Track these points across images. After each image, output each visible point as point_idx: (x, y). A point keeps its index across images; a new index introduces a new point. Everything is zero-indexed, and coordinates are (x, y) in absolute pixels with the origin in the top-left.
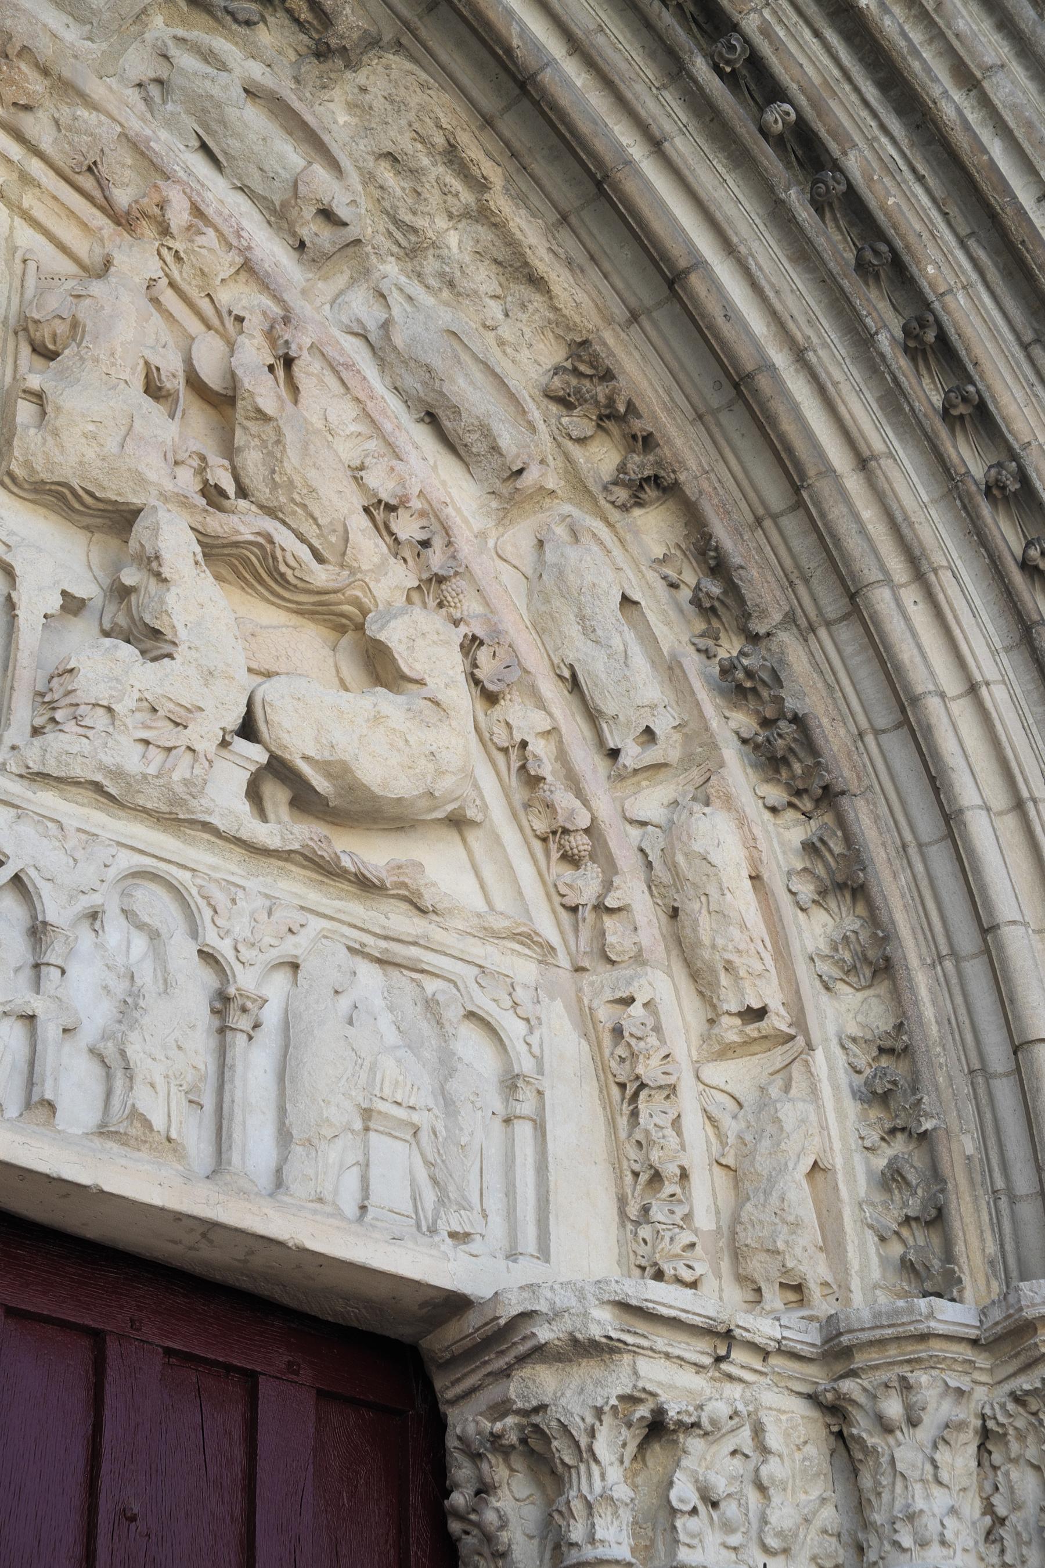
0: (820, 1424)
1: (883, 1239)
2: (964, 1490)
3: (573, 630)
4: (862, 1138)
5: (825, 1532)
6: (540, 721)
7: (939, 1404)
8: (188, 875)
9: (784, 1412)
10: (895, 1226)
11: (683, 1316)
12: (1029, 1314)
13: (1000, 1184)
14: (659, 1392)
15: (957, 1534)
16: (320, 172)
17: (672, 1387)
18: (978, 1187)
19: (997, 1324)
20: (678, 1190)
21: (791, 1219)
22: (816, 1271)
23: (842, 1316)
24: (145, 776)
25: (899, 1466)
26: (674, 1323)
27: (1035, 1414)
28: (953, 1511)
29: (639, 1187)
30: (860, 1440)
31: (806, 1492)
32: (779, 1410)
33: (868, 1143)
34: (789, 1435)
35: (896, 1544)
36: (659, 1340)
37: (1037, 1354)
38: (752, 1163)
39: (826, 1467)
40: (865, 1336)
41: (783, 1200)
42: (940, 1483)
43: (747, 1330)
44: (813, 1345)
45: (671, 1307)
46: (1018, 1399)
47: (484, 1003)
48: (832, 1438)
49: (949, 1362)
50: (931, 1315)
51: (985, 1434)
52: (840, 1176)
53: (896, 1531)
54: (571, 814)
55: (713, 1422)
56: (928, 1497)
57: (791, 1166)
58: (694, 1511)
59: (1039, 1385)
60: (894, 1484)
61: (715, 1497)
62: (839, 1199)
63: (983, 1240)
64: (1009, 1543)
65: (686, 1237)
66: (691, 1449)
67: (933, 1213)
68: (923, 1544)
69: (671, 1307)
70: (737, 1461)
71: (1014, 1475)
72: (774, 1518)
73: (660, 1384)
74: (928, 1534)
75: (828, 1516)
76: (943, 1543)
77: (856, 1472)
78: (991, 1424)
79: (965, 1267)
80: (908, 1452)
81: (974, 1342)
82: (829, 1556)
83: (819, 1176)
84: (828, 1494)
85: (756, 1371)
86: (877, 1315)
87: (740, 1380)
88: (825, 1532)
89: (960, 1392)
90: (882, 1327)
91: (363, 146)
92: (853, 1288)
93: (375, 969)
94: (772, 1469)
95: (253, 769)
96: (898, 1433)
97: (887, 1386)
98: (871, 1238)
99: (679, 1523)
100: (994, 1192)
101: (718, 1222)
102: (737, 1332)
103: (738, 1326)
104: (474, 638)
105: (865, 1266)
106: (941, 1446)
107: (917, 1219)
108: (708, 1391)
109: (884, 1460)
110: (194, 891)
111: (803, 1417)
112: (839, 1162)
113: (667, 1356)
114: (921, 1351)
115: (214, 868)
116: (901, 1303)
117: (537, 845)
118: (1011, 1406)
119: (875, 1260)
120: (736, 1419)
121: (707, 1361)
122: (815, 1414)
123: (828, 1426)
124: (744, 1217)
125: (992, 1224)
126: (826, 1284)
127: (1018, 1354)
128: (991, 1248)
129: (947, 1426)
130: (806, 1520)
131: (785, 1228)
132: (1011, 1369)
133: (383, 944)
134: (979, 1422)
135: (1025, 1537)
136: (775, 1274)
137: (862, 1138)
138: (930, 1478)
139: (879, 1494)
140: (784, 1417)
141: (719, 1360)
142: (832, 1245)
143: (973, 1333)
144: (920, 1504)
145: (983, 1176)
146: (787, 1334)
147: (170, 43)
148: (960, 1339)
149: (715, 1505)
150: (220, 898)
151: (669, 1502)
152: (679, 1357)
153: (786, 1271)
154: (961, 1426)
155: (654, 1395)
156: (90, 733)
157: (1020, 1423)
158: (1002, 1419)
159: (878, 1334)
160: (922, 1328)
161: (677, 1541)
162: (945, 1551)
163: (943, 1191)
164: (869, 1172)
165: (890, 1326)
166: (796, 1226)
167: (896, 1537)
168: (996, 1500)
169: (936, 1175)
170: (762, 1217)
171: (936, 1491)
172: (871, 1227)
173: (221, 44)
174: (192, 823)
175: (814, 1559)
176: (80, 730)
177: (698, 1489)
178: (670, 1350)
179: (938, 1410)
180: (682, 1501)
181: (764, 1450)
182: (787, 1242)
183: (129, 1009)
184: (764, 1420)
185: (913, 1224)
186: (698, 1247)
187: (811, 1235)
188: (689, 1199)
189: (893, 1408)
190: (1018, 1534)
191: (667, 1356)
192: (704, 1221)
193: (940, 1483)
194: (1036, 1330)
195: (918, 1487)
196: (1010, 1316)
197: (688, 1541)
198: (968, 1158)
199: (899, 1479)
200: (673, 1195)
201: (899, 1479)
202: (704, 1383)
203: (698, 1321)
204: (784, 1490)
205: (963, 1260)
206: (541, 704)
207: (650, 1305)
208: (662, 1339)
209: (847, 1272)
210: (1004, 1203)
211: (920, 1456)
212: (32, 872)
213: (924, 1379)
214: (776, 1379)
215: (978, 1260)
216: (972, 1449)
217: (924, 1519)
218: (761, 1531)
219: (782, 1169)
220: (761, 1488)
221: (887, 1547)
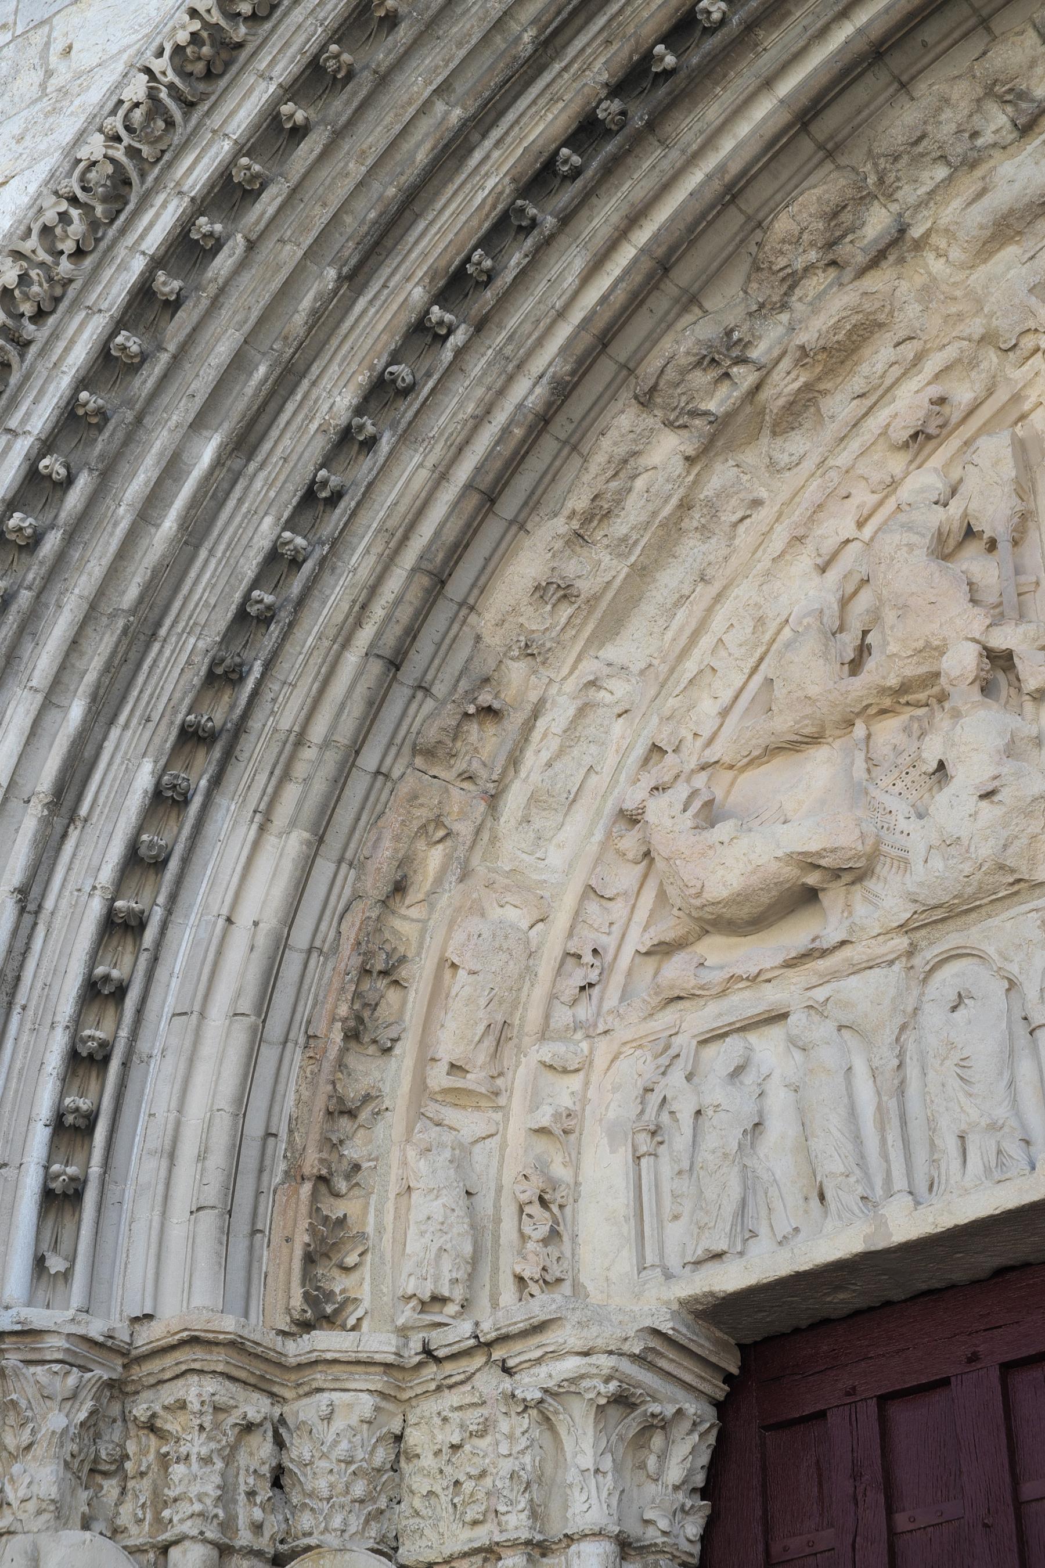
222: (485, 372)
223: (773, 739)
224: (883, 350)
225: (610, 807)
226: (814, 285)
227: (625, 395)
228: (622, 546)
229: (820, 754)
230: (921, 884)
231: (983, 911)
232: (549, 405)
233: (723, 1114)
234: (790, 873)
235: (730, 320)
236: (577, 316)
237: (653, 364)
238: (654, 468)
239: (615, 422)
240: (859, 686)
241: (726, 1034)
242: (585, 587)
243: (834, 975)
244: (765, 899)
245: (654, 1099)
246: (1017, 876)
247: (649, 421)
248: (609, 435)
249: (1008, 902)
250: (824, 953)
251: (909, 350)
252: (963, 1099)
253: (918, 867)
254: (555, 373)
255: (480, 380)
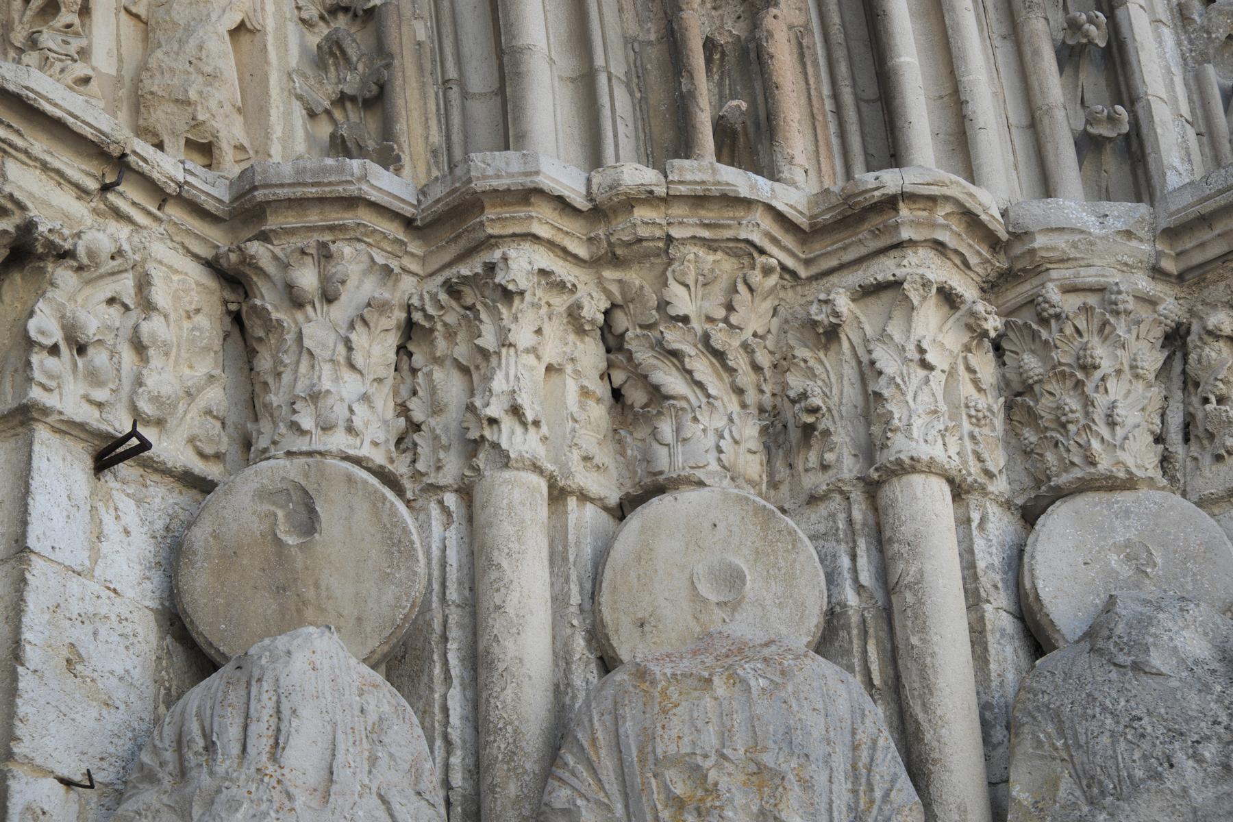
0: (216, 298)
1: (312, 115)
2: (379, 380)
4: (299, 8)
5: (209, 412)
7: (361, 281)
9: (176, 272)
10: (327, 104)
11: (70, 120)
12: (479, 185)
13: (452, 73)
14: (30, 205)
15: (367, 424)
17: (47, 204)
18: (427, 74)
19: (438, 201)
20: (75, 19)
21: (208, 69)
22: (230, 131)
23: (258, 169)
25: (307, 343)
26: (56, 127)
27: (471, 308)
28: (365, 398)
29: (29, 13)
30: (262, 313)
31: (191, 367)
32: (170, 267)
33: (305, 15)
34: (179, 298)
35: (295, 427)
36: (37, 145)
37: (482, 235)
38: (168, 12)
39: (217, 344)
40: (282, 193)
41: (201, 48)
42: (352, 366)
43: (145, 160)
44: (220, 201)
45: (56, 105)
46: (453, 290)
48: (228, 320)
49: (378, 237)
50: (364, 178)
51: (409, 329)
52: (270, 39)
53: (295, 412)
55: (91, 254)
56: (337, 379)
57: (214, 17)
58: (54, 350)
59: (479, 270)
60: (298, 362)
61: (83, 339)
62: (267, 62)
63: (427, 127)
64: (424, 449)
65: (80, 70)
66: (59, 282)
67: (374, 88)
68: (327, 428)
69: (56, 105)
70: (114, 311)
71: (438, 374)
72: (151, 381)
73: (31, 195)
74: (333, 416)
75: (215, 396)
76: (350, 429)
77: (250, 353)
78: (417, 317)
79: (405, 146)
80: (319, 329)
81: (408, 223)
82: (210, 440)
83: (245, 39)
84: (217, 372)
85: (149, 213)
86: (301, 171)
87: (129, 219)
88: (209, 412)
89: (387, 271)
90: (305, 184)
92: (273, 152)
94: (153, 327)
96: (309, 309)
97: (303, 253)
98: (298, 112)
99: (35, 359)
100: (445, 82)
101: (119, 70)
102: (132, 159)
103: (135, 152)
105: (288, 137)
106: (359, 327)
107: (353, 99)
108: (89, 222)
109: (290, 337)
111: (198, 284)
112: (270, 24)
113: (45, 167)
114: (348, 218)
116: (330, 162)
118: (443, 297)
119: (300, 134)
120: (119, 261)
121: (93, 185)
122: (211, 283)
123: (225, 303)
124: (153, 63)
125: (438, 115)
126: (240, 148)
127: (459, 236)
128: (436, 138)
129: (369, 305)
130: (189, 394)
131: (200, 79)
132: (447, 257)
134: (404, 315)
135: (444, 440)
136: (182, 126)
137: (299, 8)
138: (342, 359)
139: (279, 375)
140: (175, 278)
141: (106, 188)
142: (253, 108)
143: (409, 211)
144: (326, 384)
145: (434, 66)
146: (190, 179)
148: (394, 215)
149: (81, 349)
151: (26, 331)
152: (58, 172)
153: (196, 124)
154: (383, 307)
155: (22, 207)
157: (451, 319)
158: (431, 310)
159: (299, 192)
160: (352, 190)
161: (30, 380)
162: (350, 440)
163: (388, 66)
164: (303, 48)
165: (313, 185)
166: (212, 78)
167: (295, 418)
168: (413, 404)
169: (381, 51)
170: (173, 65)
171: (348, 375)
172: (300, 98)
175: (192, 440)
177: (64, 327)
178: (48, 159)
179: (360, 286)
180: (42, 333)
181: (148, 306)
182: (201, 93)
184: (153, 272)
185: (349, 105)
186: (93, 83)
187: (228, 91)
188: (89, 36)
189: (307, 278)
190: (436, 438)
191: (45, 167)
192: (103, 61)
193: (352, 366)
194: (482, 210)
195: (327, 369)
196: (454, 191)
197: (44, 380)
198: (419, 44)
199: (305, 357)
200: (69, 26)
201: (305, 357)
202: (86, 212)
203: (87, 132)
204: (167, 354)
205: (403, 139)
207: (31, 95)
208: (39, 144)
209: (267, 136)
210: (454, 94)
211: (332, 337)
213: (347, 250)
214: (171, 230)
215: (420, 147)
216: (393, 340)
217: (330, 401)
218: (134, 392)
219: (205, 19)
220: (139, 347)
221: (283, 429)
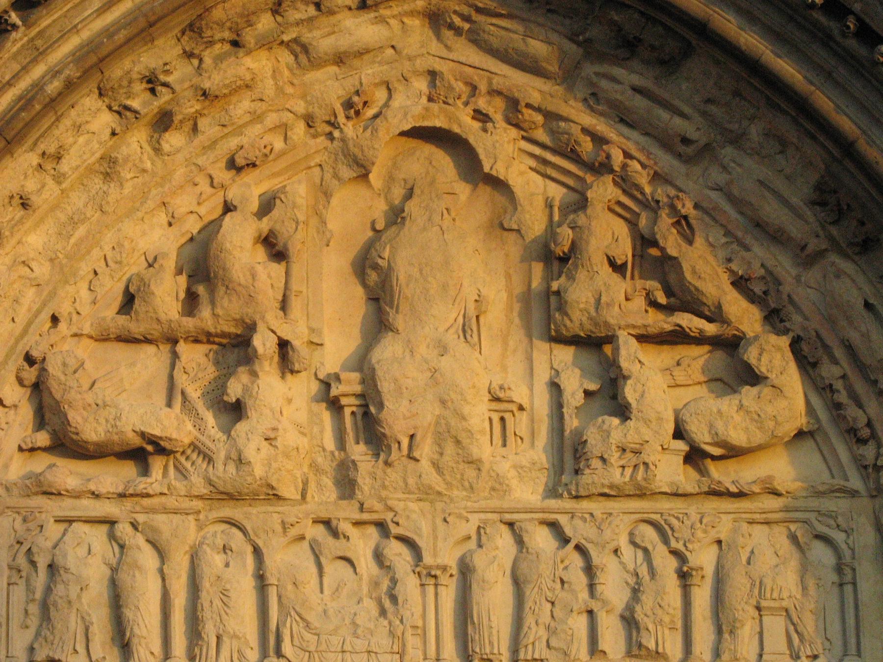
3: (843, 323)
6: (836, 371)
8: (659, 516)
16: (678, 121)
24: (625, 483)
47: (822, 529)
54: (855, 420)
91: (697, 99)
93: (765, 528)
95: (684, 454)
104: (799, 336)
110: (663, 523)
115: (672, 509)
117: (846, 435)
133: (764, 516)
147: (593, 76)
150: (674, 522)
156: (596, 472)
173: (617, 71)
174: (655, 493)
176: (591, 471)
183: (636, 592)
206: (836, 362)
212: (583, 542)
222: (19, 52)
223: (126, 333)
224: (244, 102)
225: (21, 349)
226: (218, 48)
227: (93, 85)
228: (59, 178)
229: (151, 349)
230: (219, 478)
231: (248, 502)
232: (60, 94)
233: (70, 576)
234: (137, 441)
235: (167, 59)
236: (86, 34)
237: (116, 71)
238: (94, 133)
239: (82, 101)
240: (189, 323)
241: (74, 521)
242: (35, 199)
243: (153, 511)
244: (117, 449)
245: (24, 548)
246: (275, 492)
247: (100, 103)
248: (76, 108)
249: (262, 502)
250: (148, 495)
251: (260, 107)
252: (223, 612)
253: (220, 467)
254: (69, 75)
255: (14, 57)
